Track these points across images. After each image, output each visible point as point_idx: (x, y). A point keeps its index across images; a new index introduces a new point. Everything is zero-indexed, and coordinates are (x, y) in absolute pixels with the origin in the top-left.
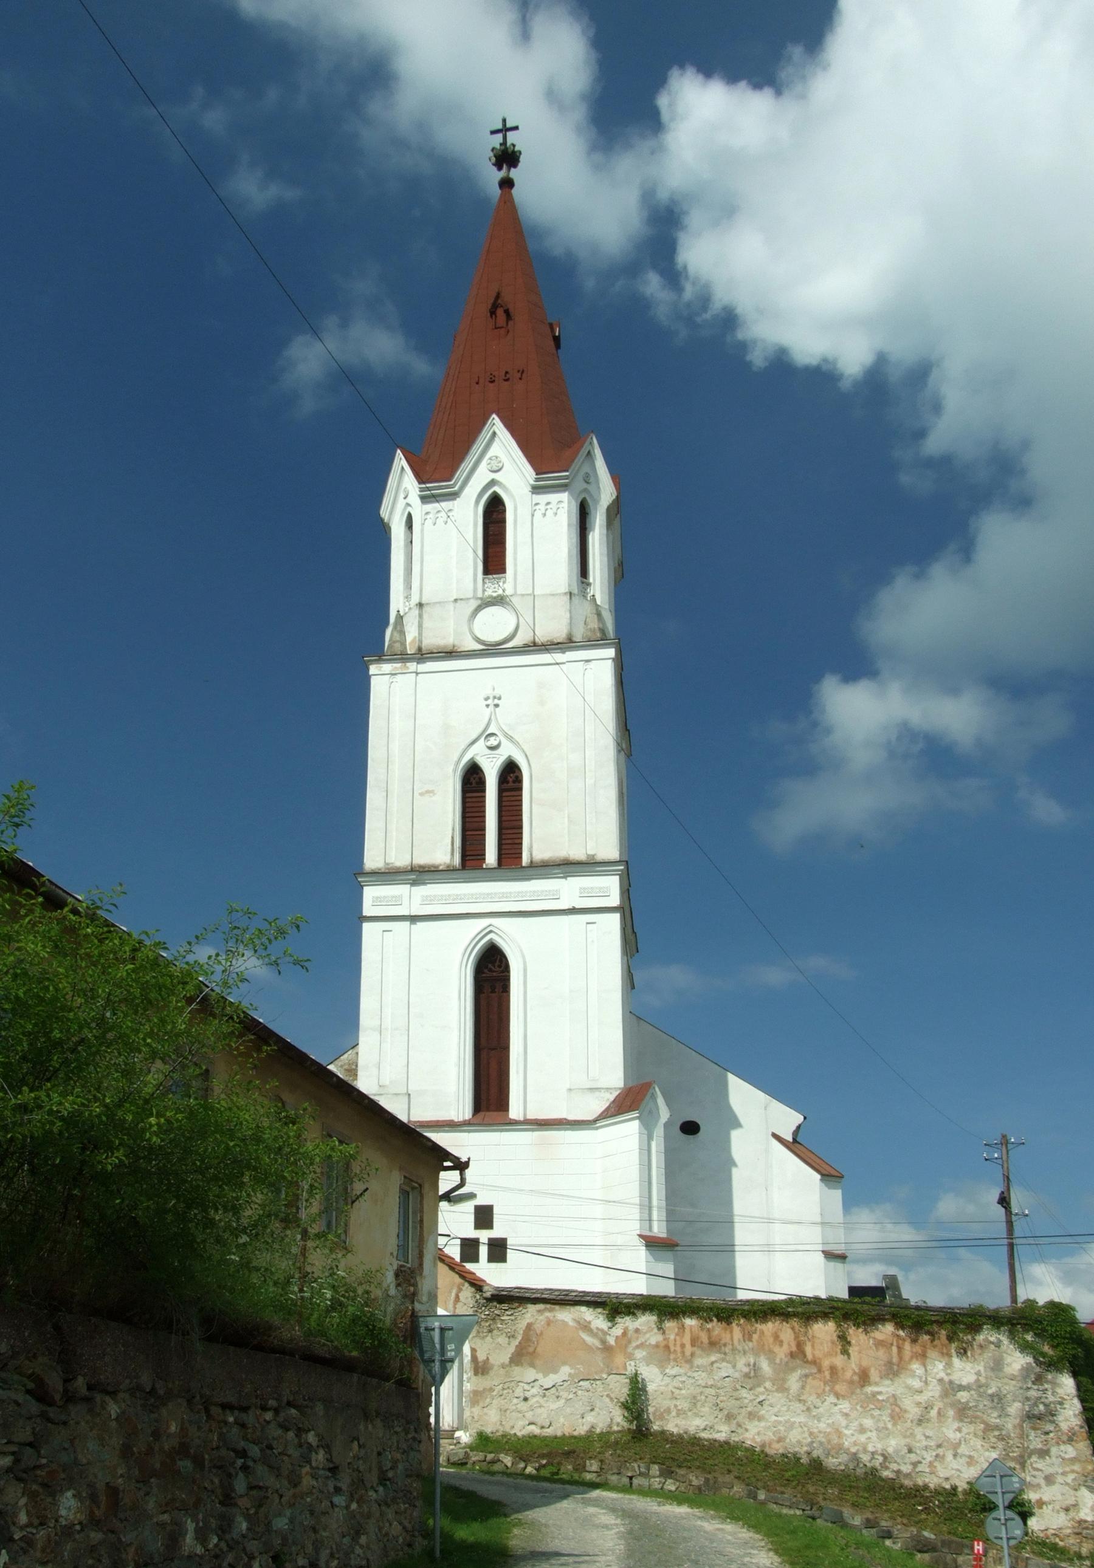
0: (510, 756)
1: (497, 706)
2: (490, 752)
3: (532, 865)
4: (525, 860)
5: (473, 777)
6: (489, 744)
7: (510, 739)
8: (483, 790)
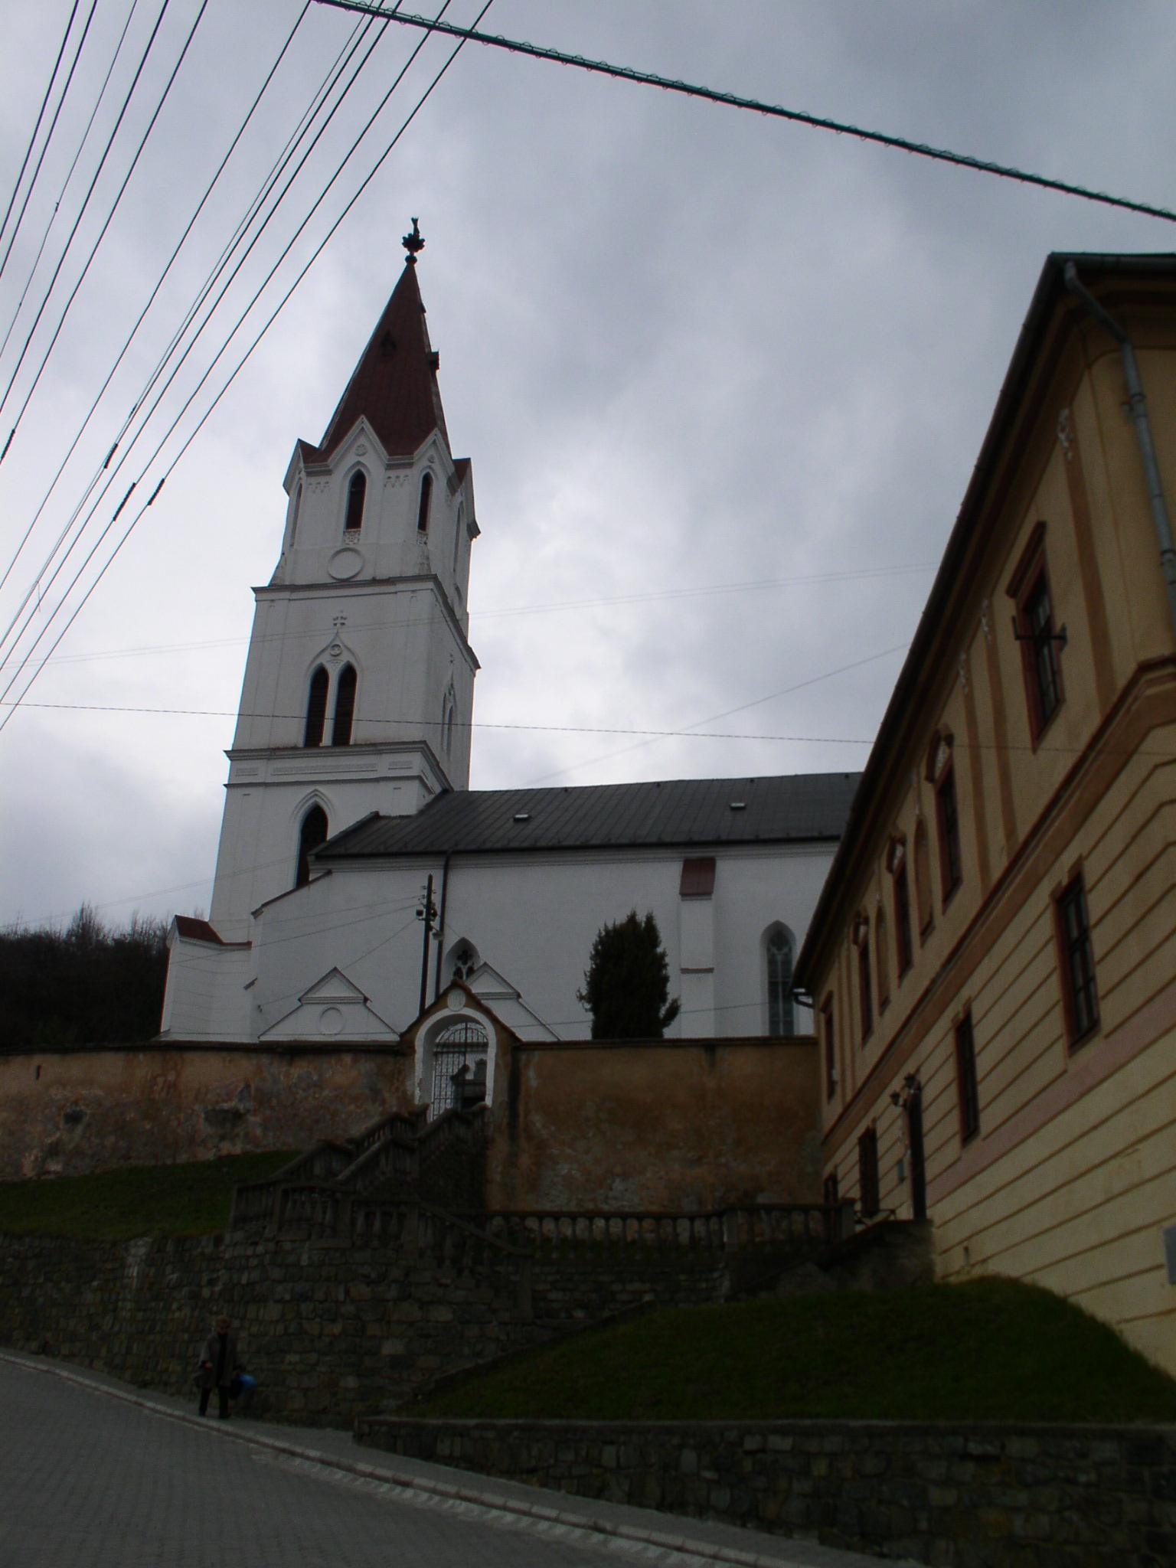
0: (348, 662)
1: (343, 624)
2: (334, 658)
3: (355, 745)
4: (352, 742)
5: (320, 678)
6: (333, 653)
7: (349, 650)
8: (326, 687)
